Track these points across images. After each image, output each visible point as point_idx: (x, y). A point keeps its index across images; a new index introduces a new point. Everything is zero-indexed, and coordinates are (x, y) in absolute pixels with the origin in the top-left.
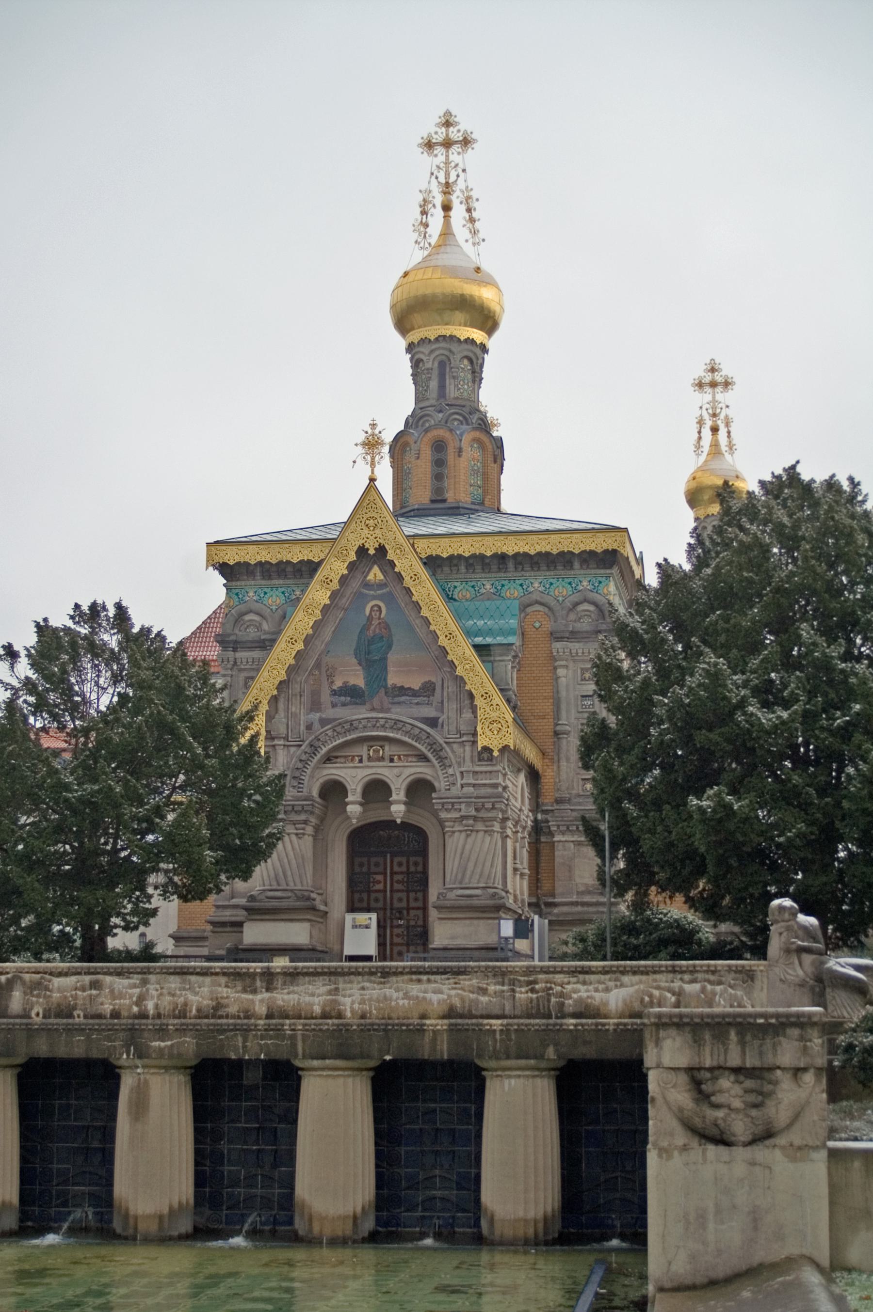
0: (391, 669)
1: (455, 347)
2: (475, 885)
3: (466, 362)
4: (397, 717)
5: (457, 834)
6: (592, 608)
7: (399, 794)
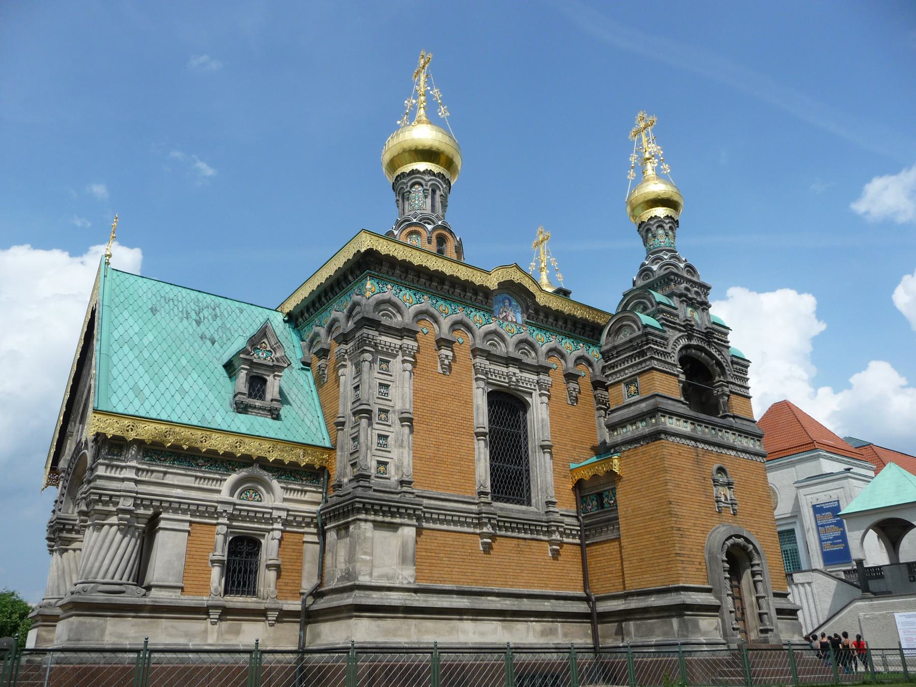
3: (417, 186)
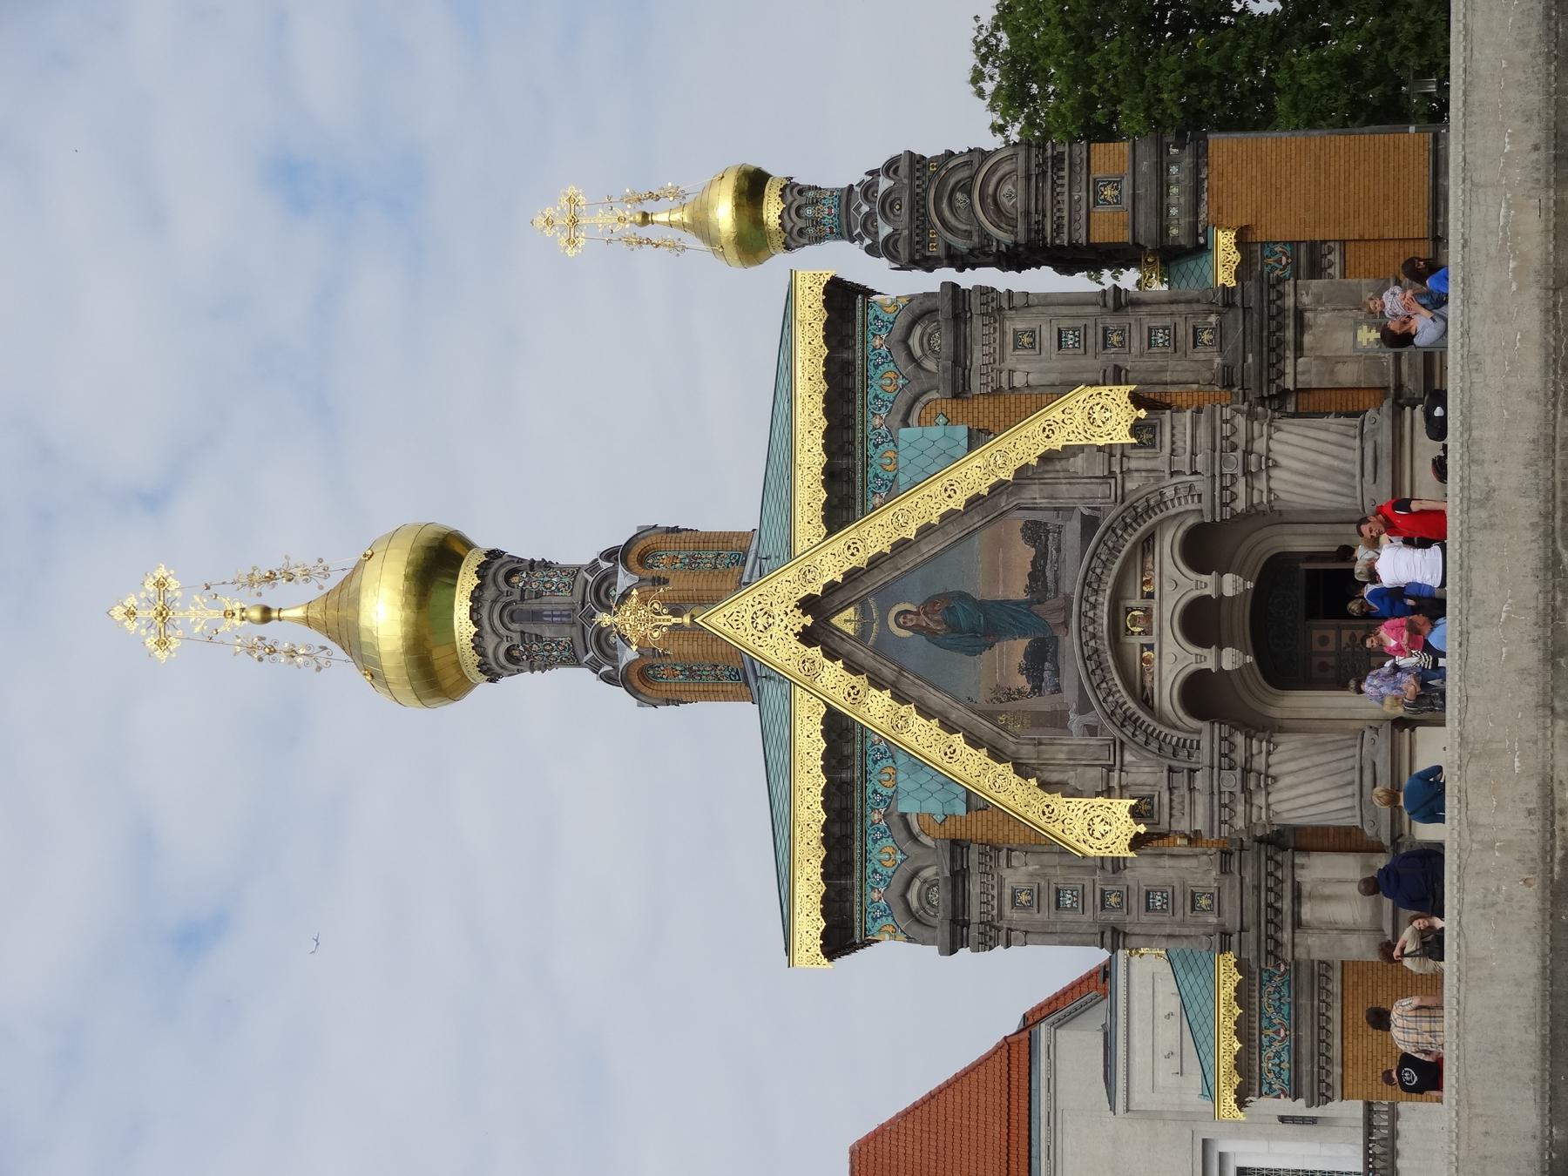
0: (1000, 595)
1: (489, 593)
2: (1358, 453)
3: (515, 580)
4: (1078, 588)
5: (1273, 484)
6: (918, 331)
7: (1206, 585)
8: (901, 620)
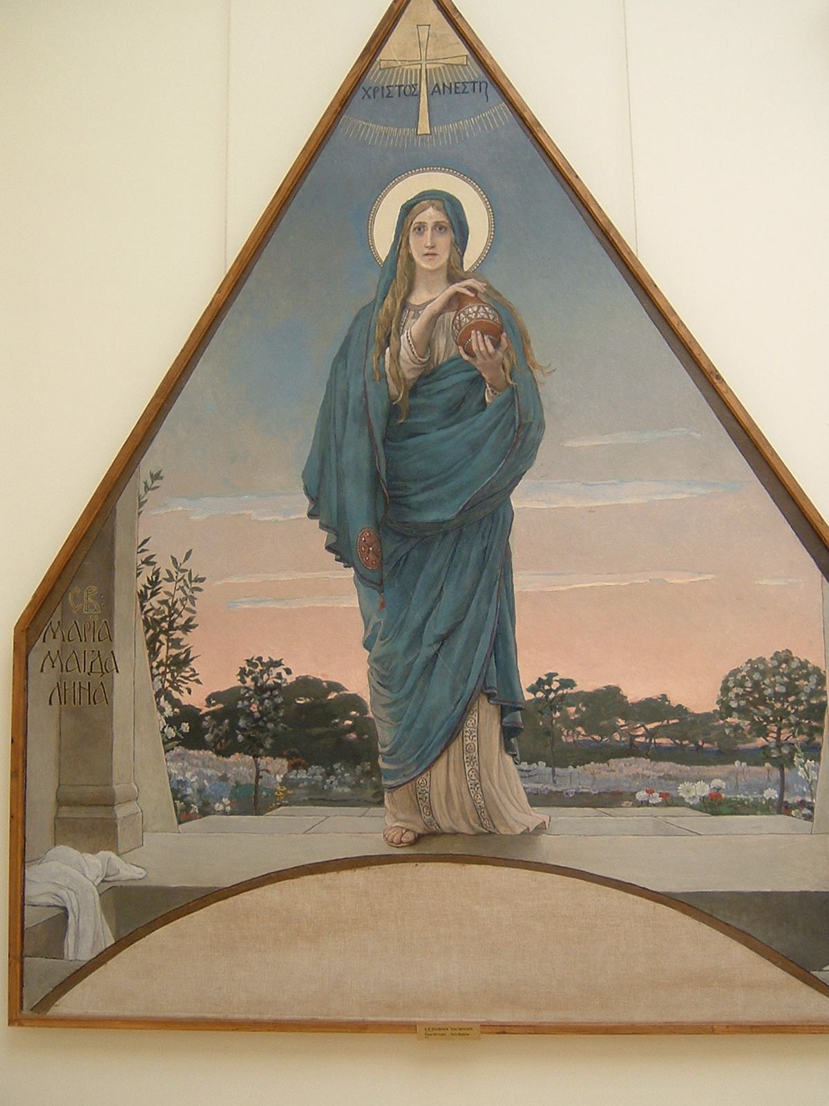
8: (430, 215)
